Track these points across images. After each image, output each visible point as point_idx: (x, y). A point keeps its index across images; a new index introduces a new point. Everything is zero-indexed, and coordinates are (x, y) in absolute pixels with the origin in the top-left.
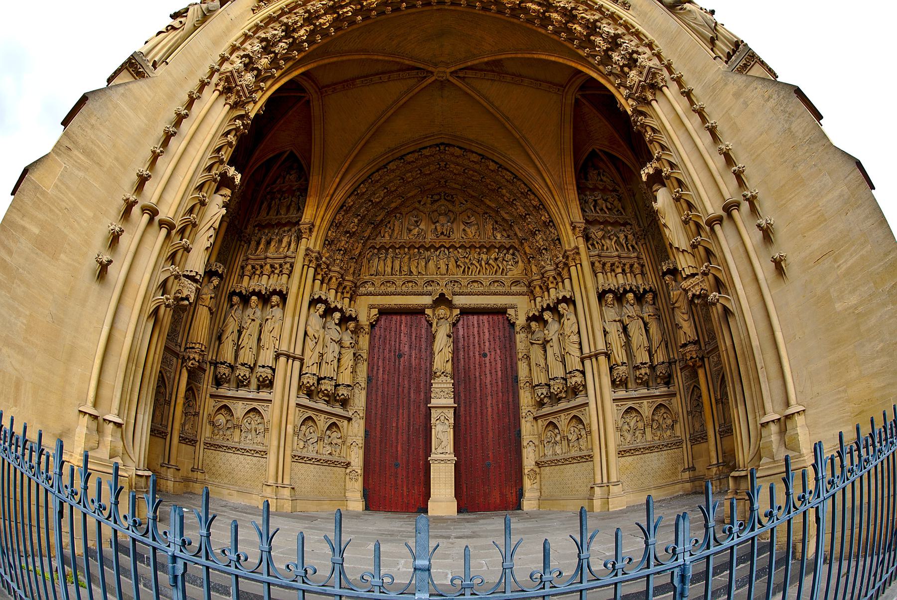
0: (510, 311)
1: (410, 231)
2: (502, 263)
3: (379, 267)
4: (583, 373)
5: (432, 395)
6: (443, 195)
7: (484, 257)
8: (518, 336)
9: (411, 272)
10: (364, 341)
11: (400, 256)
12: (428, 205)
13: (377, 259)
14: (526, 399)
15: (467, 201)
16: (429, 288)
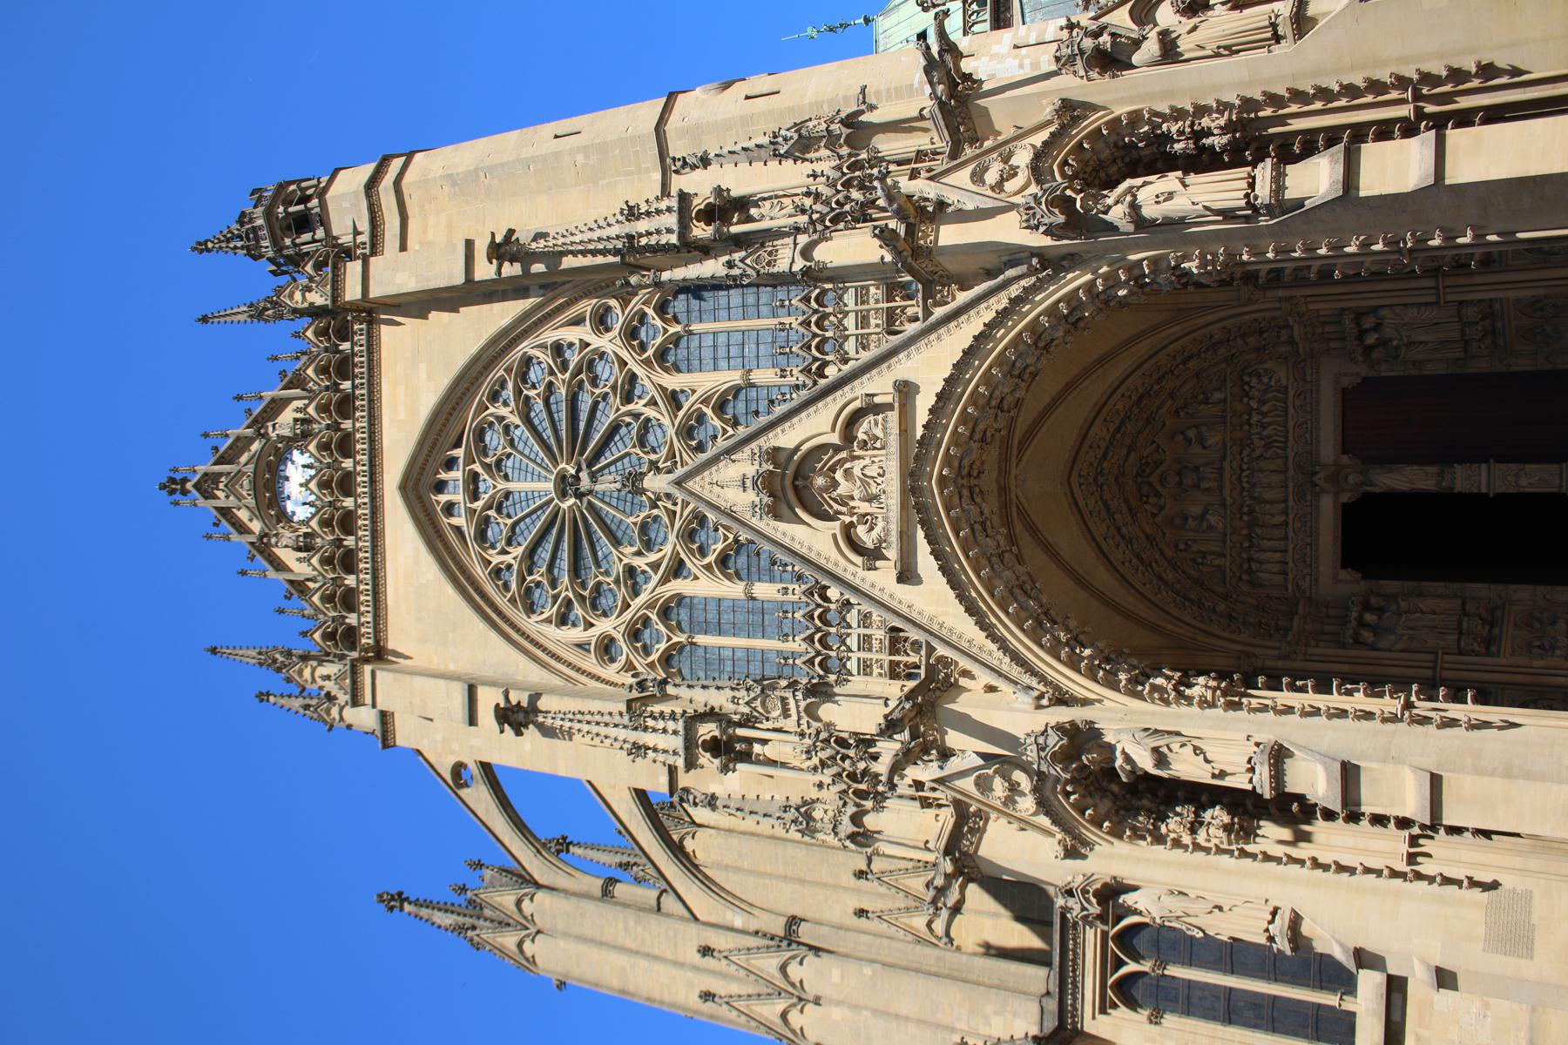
0: (1346, 382)
1: (1210, 527)
2: (1265, 392)
3: (1274, 570)
4: (1461, 302)
5: (1475, 491)
6: (1139, 479)
7: (1255, 418)
8: (1384, 374)
9: (1281, 525)
11: (1255, 541)
12: (1162, 502)
13: (1260, 574)
14: (1481, 366)
15: (1153, 442)
16: (1309, 498)
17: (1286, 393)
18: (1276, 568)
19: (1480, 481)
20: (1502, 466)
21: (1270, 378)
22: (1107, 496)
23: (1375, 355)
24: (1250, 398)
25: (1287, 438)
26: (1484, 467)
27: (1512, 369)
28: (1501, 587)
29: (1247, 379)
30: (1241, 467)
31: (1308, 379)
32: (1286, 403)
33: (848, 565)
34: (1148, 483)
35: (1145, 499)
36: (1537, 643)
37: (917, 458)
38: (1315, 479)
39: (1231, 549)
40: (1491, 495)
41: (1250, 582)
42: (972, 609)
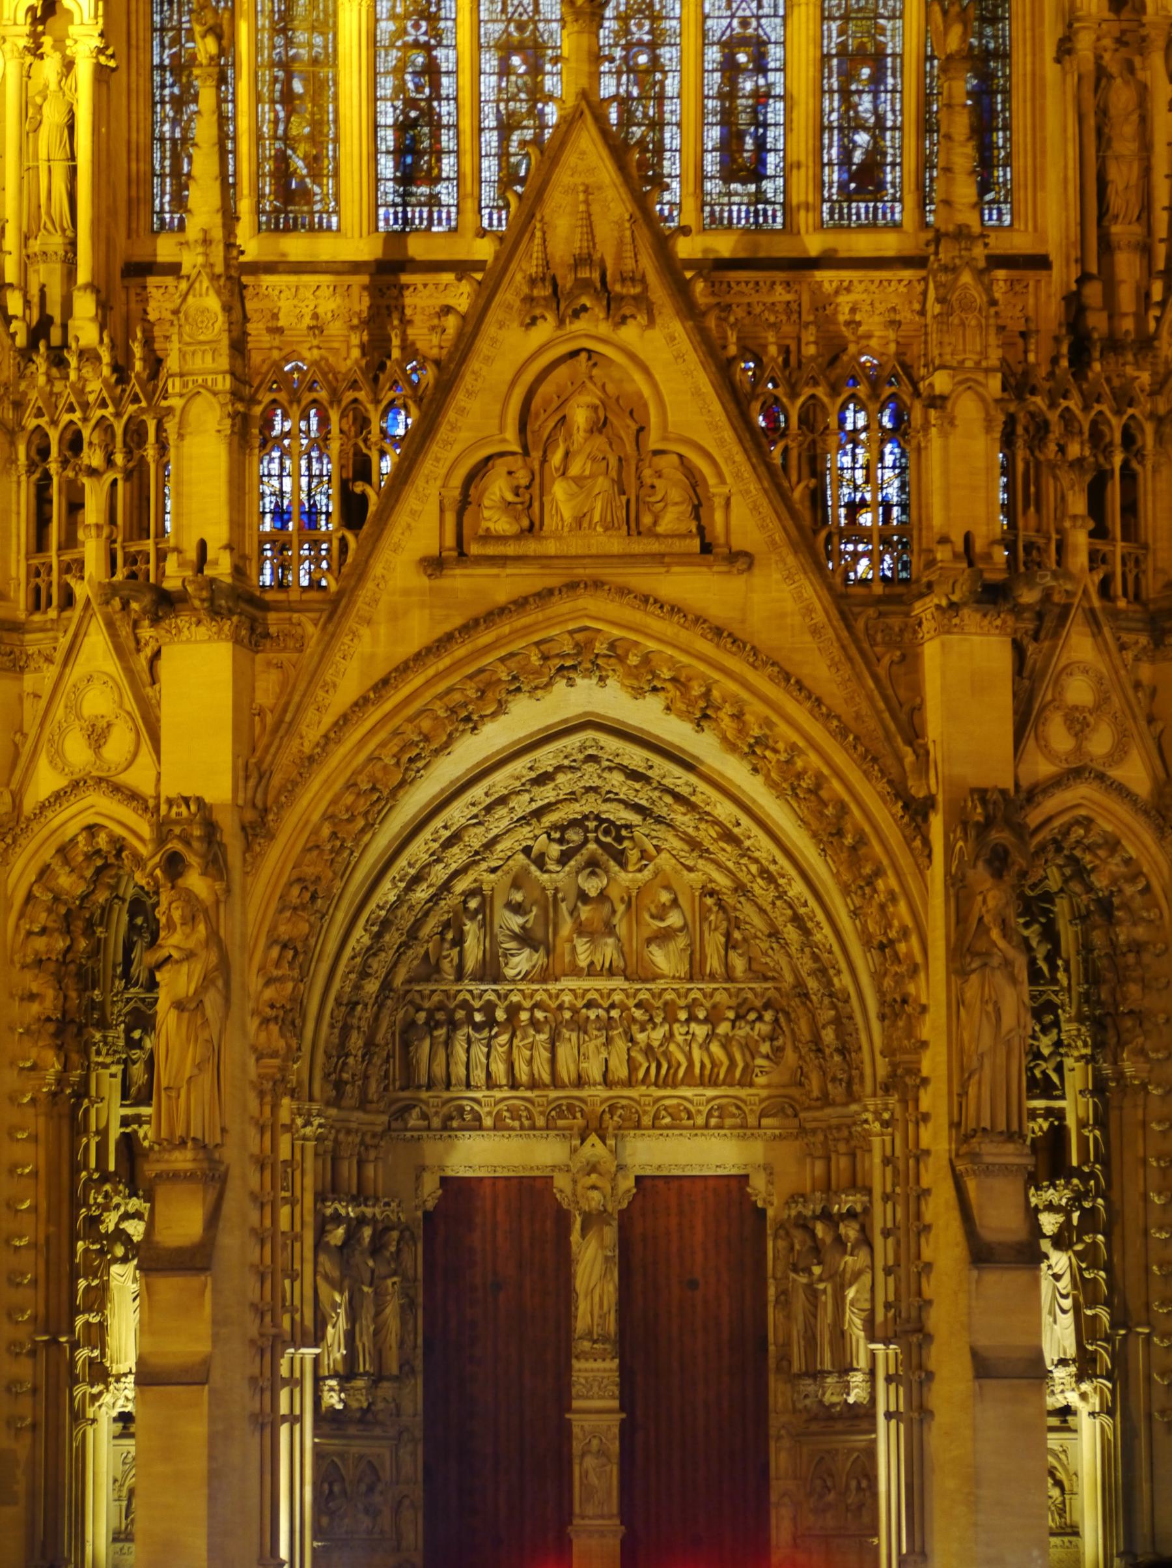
5: (574, 1391)
7: (700, 1031)
10: (415, 1259)
12: (552, 866)
17: (741, 1084)
18: (439, 1070)
19: (592, 1398)
20: (616, 1430)
21: (767, 1057)
22: (561, 778)
23: (798, 1236)
24: (733, 1022)
25: (665, 1085)
26: (615, 1404)
27: (772, 1444)
28: (419, 1433)
29: (768, 1016)
30: (613, 1006)
31: (764, 1121)
32: (724, 1083)
33: (448, 464)
34: (586, 841)
35: (557, 835)
36: (336, 1488)
37: (623, 591)
38: (593, 1138)
39: (470, 991)
40: (568, 1416)
41: (411, 1024)
42: (384, 684)
